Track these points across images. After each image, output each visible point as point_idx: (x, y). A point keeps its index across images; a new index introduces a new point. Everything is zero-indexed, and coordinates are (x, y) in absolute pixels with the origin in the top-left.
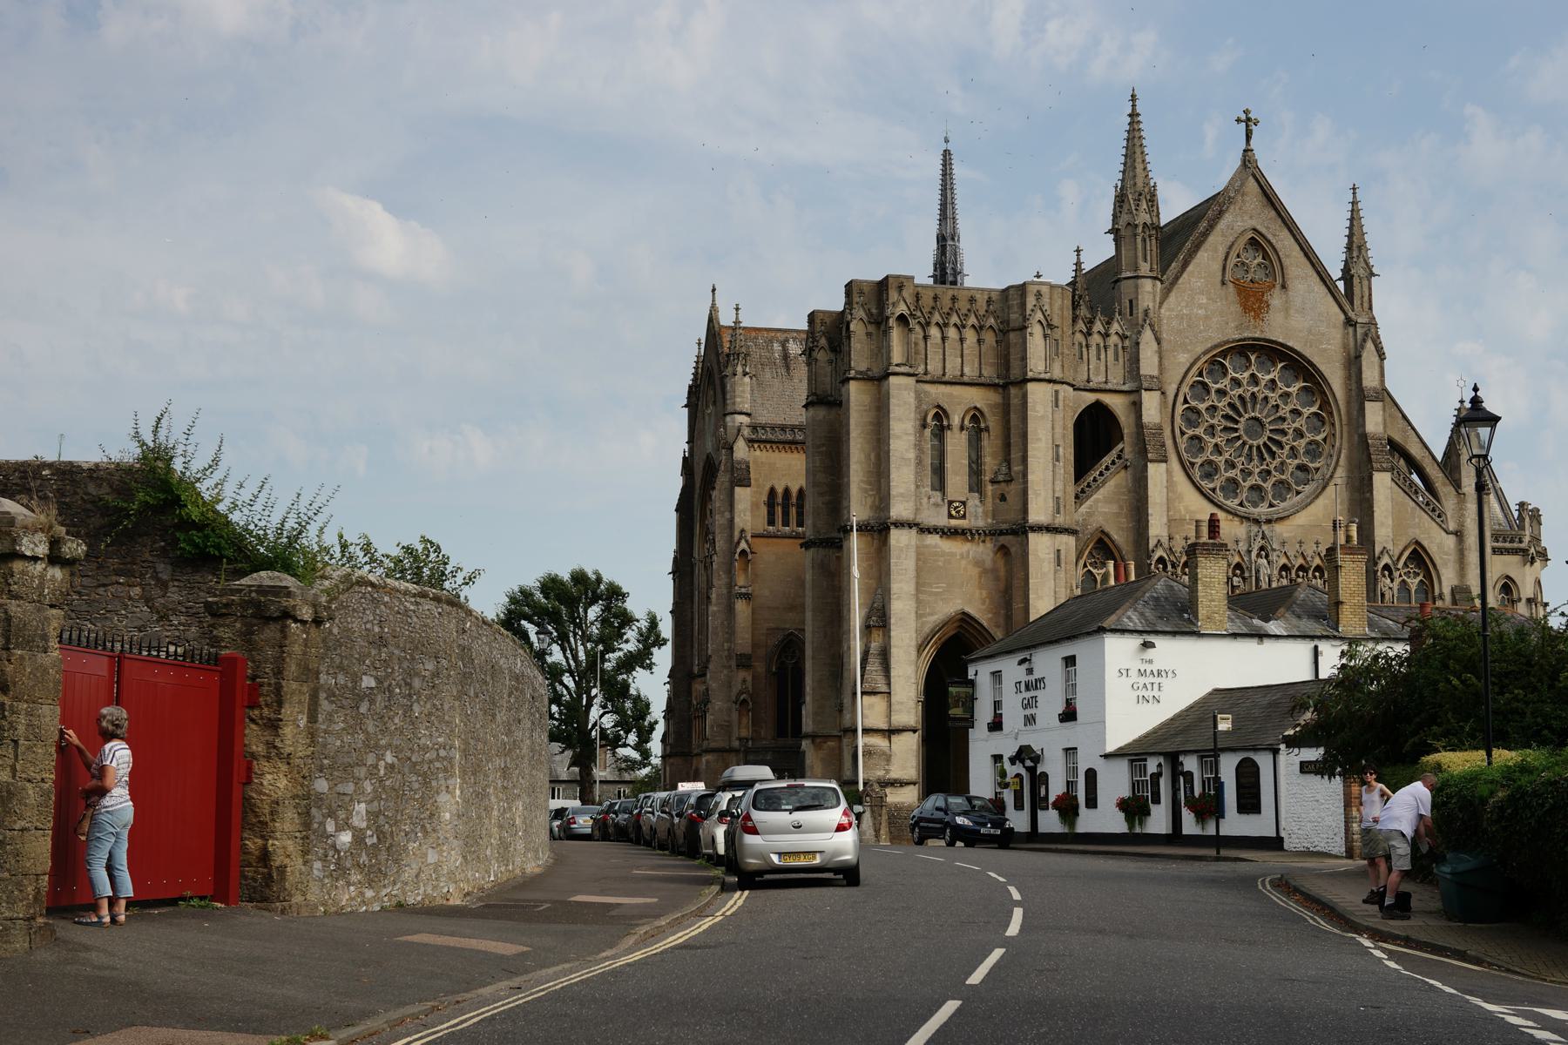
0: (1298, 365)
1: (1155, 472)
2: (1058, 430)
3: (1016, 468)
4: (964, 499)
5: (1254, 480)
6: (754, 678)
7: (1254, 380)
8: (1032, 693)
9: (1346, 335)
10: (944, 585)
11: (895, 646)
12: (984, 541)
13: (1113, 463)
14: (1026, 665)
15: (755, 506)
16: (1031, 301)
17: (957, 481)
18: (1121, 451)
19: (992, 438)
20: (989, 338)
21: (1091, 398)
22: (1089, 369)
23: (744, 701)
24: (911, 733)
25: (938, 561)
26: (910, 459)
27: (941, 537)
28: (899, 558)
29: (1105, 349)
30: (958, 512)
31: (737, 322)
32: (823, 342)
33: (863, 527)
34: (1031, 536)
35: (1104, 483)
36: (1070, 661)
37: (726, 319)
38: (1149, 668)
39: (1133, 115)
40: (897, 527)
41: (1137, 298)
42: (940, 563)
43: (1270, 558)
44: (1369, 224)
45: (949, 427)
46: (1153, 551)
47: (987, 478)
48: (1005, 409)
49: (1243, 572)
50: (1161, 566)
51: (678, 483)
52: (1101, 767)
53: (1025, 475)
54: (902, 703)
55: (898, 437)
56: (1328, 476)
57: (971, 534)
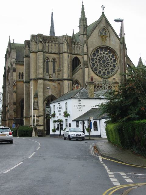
0: (111, 51)
1: (86, 69)
2: (69, 62)
3: (62, 69)
5: (104, 71)
6: (17, 107)
7: (104, 53)
8: (60, 109)
9: (120, 45)
13: (79, 68)
14: (59, 104)
15: (17, 76)
17: (51, 71)
20: (57, 45)
21: (75, 56)
23: (15, 111)
31: (13, 42)
32: (27, 46)
35: (77, 71)
36: (66, 103)
37: (12, 42)
38: (80, 105)
39: (83, 6)
45: (49, 61)
51: (3, 72)
52: (71, 123)
53: (63, 70)
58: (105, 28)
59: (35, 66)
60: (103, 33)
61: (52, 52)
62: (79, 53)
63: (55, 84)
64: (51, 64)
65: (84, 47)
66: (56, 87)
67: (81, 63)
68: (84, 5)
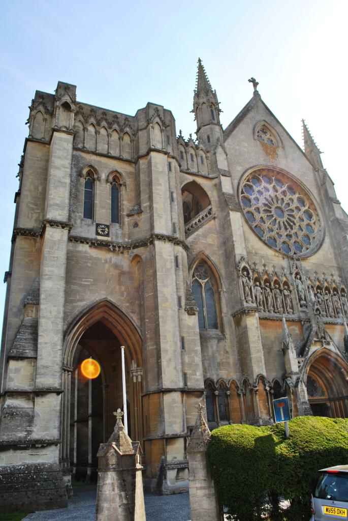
0: (295, 186)
3: (145, 204)
4: (108, 224)
5: (284, 238)
9: (315, 175)
10: (92, 280)
11: (44, 317)
12: (122, 253)
13: (206, 216)
16: (152, 112)
17: (103, 213)
18: (211, 209)
19: (128, 190)
20: (127, 139)
21: (191, 178)
22: (187, 164)
24: (54, 395)
25: (87, 263)
26: (66, 183)
27: (90, 246)
28: (52, 248)
29: (196, 156)
30: (103, 231)
33: (27, 232)
34: (157, 243)
35: (202, 226)
40: (51, 226)
41: (212, 134)
42: (89, 265)
43: (302, 280)
44: (312, 134)
45: (99, 179)
46: (239, 263)
47: (125, 213)
48: (136, 176)
49: (289, 287)
50: (245, 273)
53: (151, 207)
54: (47, 367)
55: (58, 168)
57: (113, 246)
58: (266, 124)
59: (40, 188)
60: (266, 137)
61: (108, 153)
62: (204, 172)
63: (124, 260)
64: (103, 192)
65: (217, 155)
66: (122, 273)
68: (202, 63)
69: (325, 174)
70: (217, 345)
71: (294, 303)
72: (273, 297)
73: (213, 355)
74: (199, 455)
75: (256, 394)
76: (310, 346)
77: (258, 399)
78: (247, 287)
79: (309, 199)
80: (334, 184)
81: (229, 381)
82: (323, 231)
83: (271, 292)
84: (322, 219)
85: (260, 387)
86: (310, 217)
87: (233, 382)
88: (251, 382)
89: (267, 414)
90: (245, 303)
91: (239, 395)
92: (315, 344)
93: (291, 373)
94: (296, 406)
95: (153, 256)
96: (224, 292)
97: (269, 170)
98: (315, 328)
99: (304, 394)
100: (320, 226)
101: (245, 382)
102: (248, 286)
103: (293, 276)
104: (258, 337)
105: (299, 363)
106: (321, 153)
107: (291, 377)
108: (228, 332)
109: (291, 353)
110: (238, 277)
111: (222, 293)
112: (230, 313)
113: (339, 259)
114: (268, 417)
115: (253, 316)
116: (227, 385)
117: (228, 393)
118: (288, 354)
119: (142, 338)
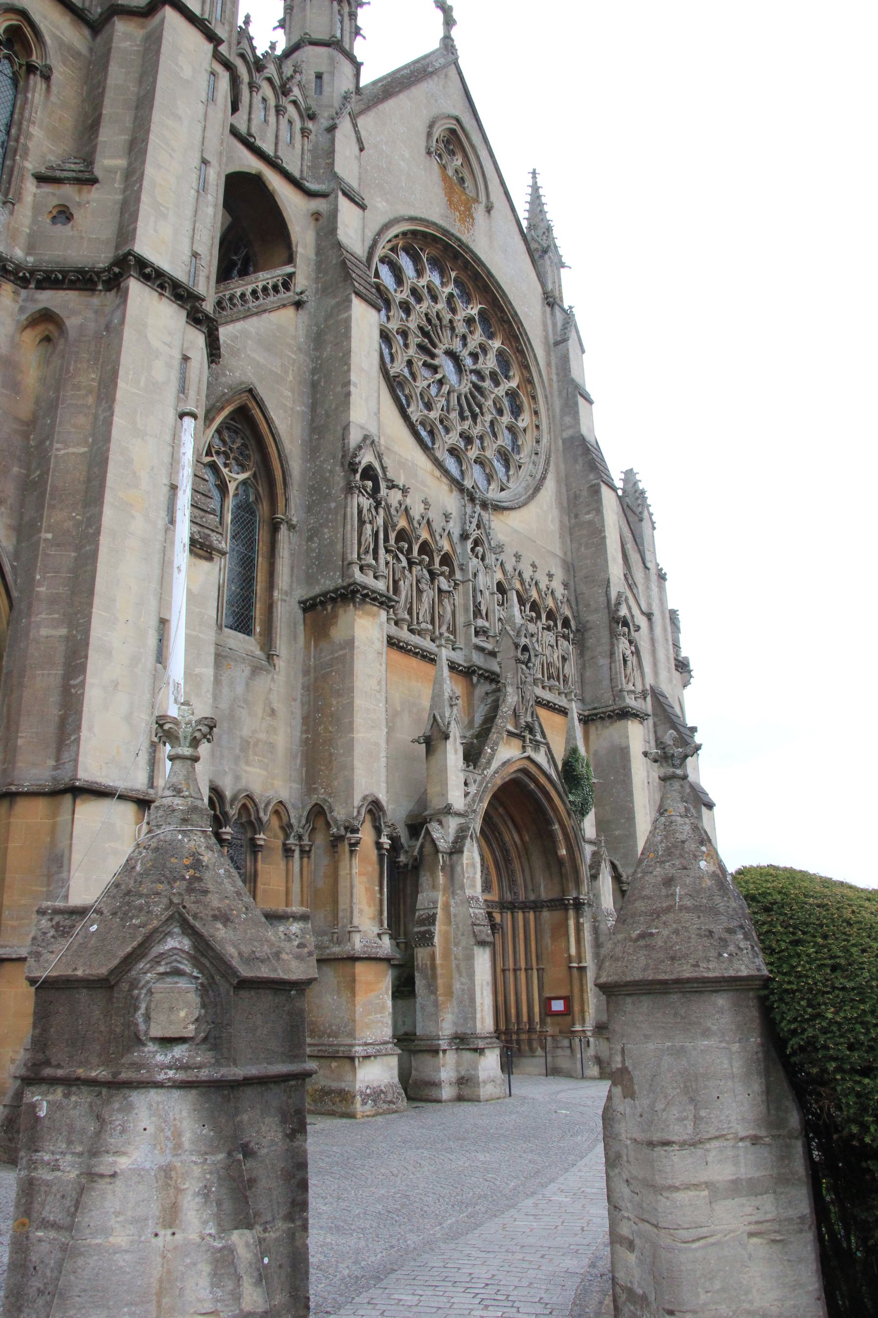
9: (544, 313)
13: (275, 288)
18: (291, 276)
19: (53, 99)
21: (252, 164)
34: (135, 287)
41: (332, 73)
43: (487, 561)
49: (452, 572)
50: (370, 484)
56: (538, 477)
67: (299, 260)
69: (569, 318)
70: (247, 684)
71: (460, 620)
72: (411, 585)
73: (232, 710)
74: (721, 1001)
75: (352, 852)
76: (497, 744)
77: (355, 870)
78: (368, 527)
79: (525, 366)
80: (583, 352)
81: (267, 805)
82: (543, 457)
83: (410, 571)
84: (544, 426)
85: (366, 835)
86: (516, 411)
87: (280, 808)
88: (340, 814)
89: (374, 919)
90: (356, 569)
91: (287, 851)
92: (508, 743)
93: (448, 810)
94: (447, 906)
95: (107, 328)
96: (291, 527)
97: (447, 247)
98: (511, 698)
99: (475, 873)
100: (538, 442)
101: (318, 813)
102: (371, 522)
103: (469, 544)
104: (379, 683)
105: (466, 784)
106: (563, 266)
107: (440, 823)
108: (282, 646)
109: (453, 752)
110: (349, 489)
111: (283, 528)
112: (302, 592)
113: (569, 542)
114: (376, 930)
115: (374, 615)
116: (262, 814)
117: (261, 838)
118: (445, 752)
119: (15, 594)
